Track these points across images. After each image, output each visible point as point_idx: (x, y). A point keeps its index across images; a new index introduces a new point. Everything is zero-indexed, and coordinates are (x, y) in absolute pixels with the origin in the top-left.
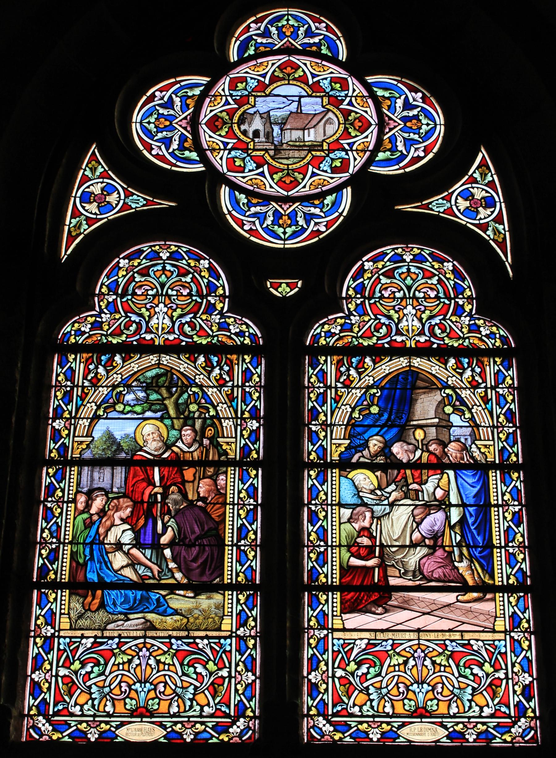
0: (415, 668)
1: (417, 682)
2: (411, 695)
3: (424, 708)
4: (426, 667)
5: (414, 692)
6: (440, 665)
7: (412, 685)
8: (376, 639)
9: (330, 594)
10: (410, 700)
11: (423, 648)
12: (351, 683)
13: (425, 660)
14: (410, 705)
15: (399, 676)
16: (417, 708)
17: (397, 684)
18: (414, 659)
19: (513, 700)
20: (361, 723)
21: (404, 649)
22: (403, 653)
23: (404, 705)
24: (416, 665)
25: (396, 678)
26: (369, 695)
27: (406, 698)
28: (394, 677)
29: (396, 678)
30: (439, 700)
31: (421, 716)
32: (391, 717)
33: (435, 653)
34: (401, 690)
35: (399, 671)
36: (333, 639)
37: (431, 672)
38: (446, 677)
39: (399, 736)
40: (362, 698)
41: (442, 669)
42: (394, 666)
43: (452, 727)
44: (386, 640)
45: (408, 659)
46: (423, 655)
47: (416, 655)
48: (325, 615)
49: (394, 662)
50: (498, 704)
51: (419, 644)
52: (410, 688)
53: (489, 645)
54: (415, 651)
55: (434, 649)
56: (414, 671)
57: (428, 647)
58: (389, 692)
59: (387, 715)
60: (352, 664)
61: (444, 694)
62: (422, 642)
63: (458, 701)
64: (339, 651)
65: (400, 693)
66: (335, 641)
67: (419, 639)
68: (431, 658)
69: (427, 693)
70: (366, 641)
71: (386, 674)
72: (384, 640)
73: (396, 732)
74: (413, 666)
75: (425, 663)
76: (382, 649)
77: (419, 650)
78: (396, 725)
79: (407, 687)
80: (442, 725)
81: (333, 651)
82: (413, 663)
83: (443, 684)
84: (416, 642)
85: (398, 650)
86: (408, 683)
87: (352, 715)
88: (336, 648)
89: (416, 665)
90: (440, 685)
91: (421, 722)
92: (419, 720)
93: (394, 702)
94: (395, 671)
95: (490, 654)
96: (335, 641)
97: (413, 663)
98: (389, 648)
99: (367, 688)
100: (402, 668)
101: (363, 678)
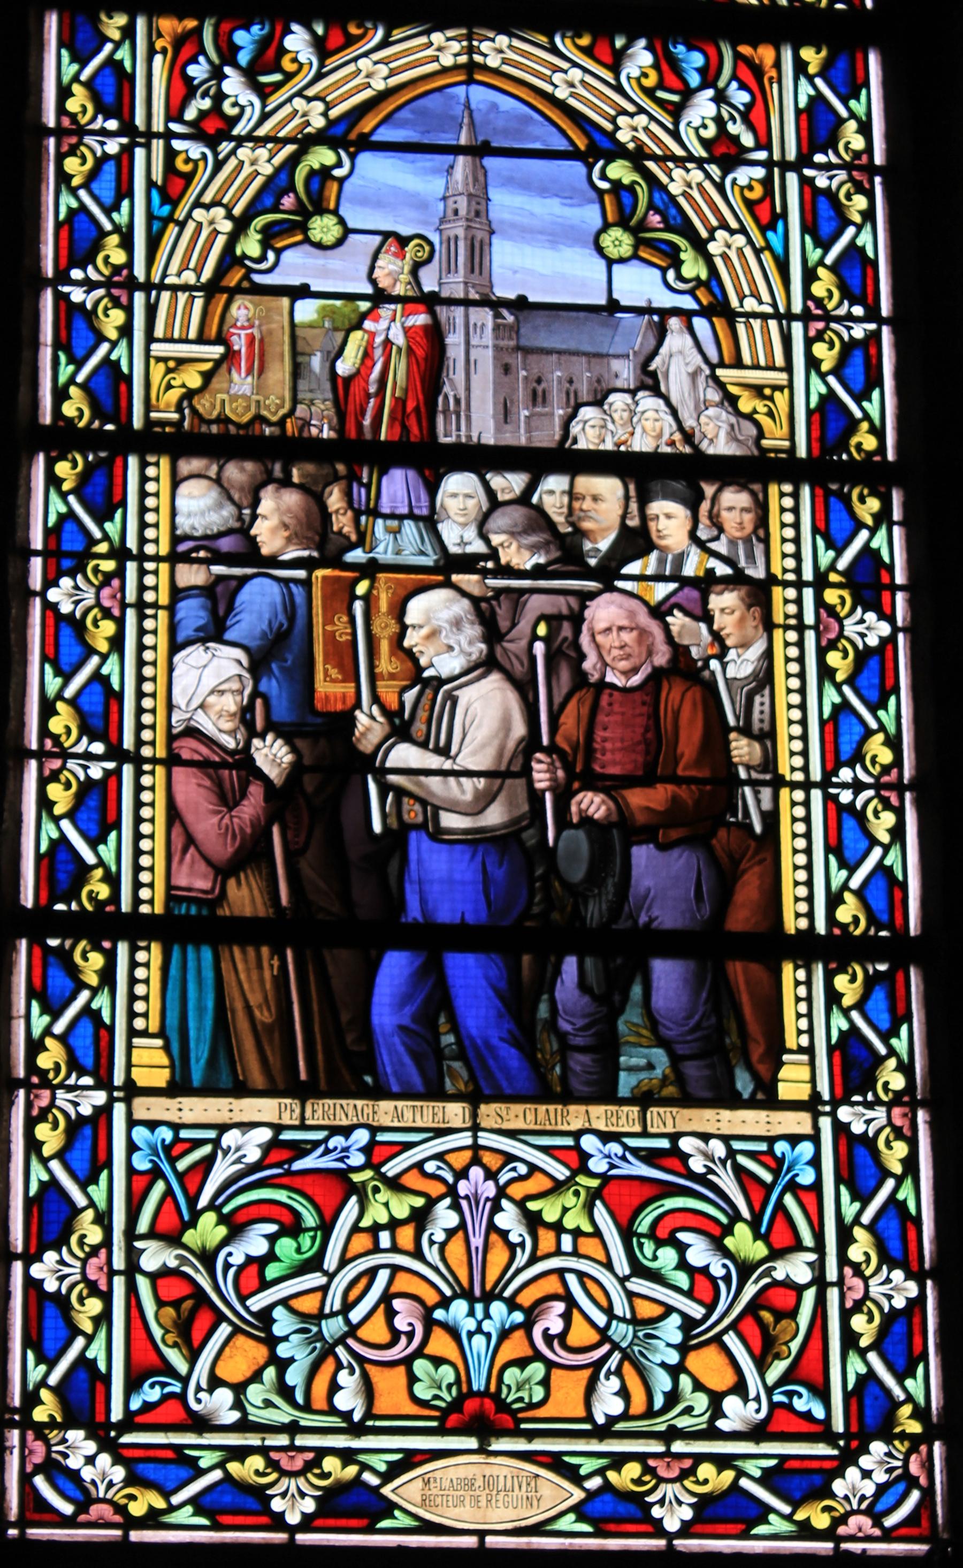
0: (458, 1239)
6: (558, 1228)
8: (303, 1127)
13: (497, 1208)
16: (465, 1395)
19: (843, 1371)
20: (240, 1454)
22: (411, 1180)
24: (462, 1225)
26: (272, 1342)
32: (358, 1430)
33: (537, 1184)
37: (521, 1258)
41: (567, 1242)
42: (375, 1229)
43: (601, 1472)
49: (377, 1214)
50: (781, 1382)
51: (476, 1147)
54: (462, 1174)
55: (533, 1169)
56: (456, 1249)
57: (510, 1158)
61: (572, 1340)
62: (485, 1139)
67: (475, 1128)
68: (520, 1204)
72: (335, 1130)
74: (450, 1233)
76: (327, 1163)
77: (476, 1173)
80: (555, 1462)
82: (452, 1219)
84: (465, 1139)
89: (462, 1225)
97: (452, 1219)
101: (250, 1280)
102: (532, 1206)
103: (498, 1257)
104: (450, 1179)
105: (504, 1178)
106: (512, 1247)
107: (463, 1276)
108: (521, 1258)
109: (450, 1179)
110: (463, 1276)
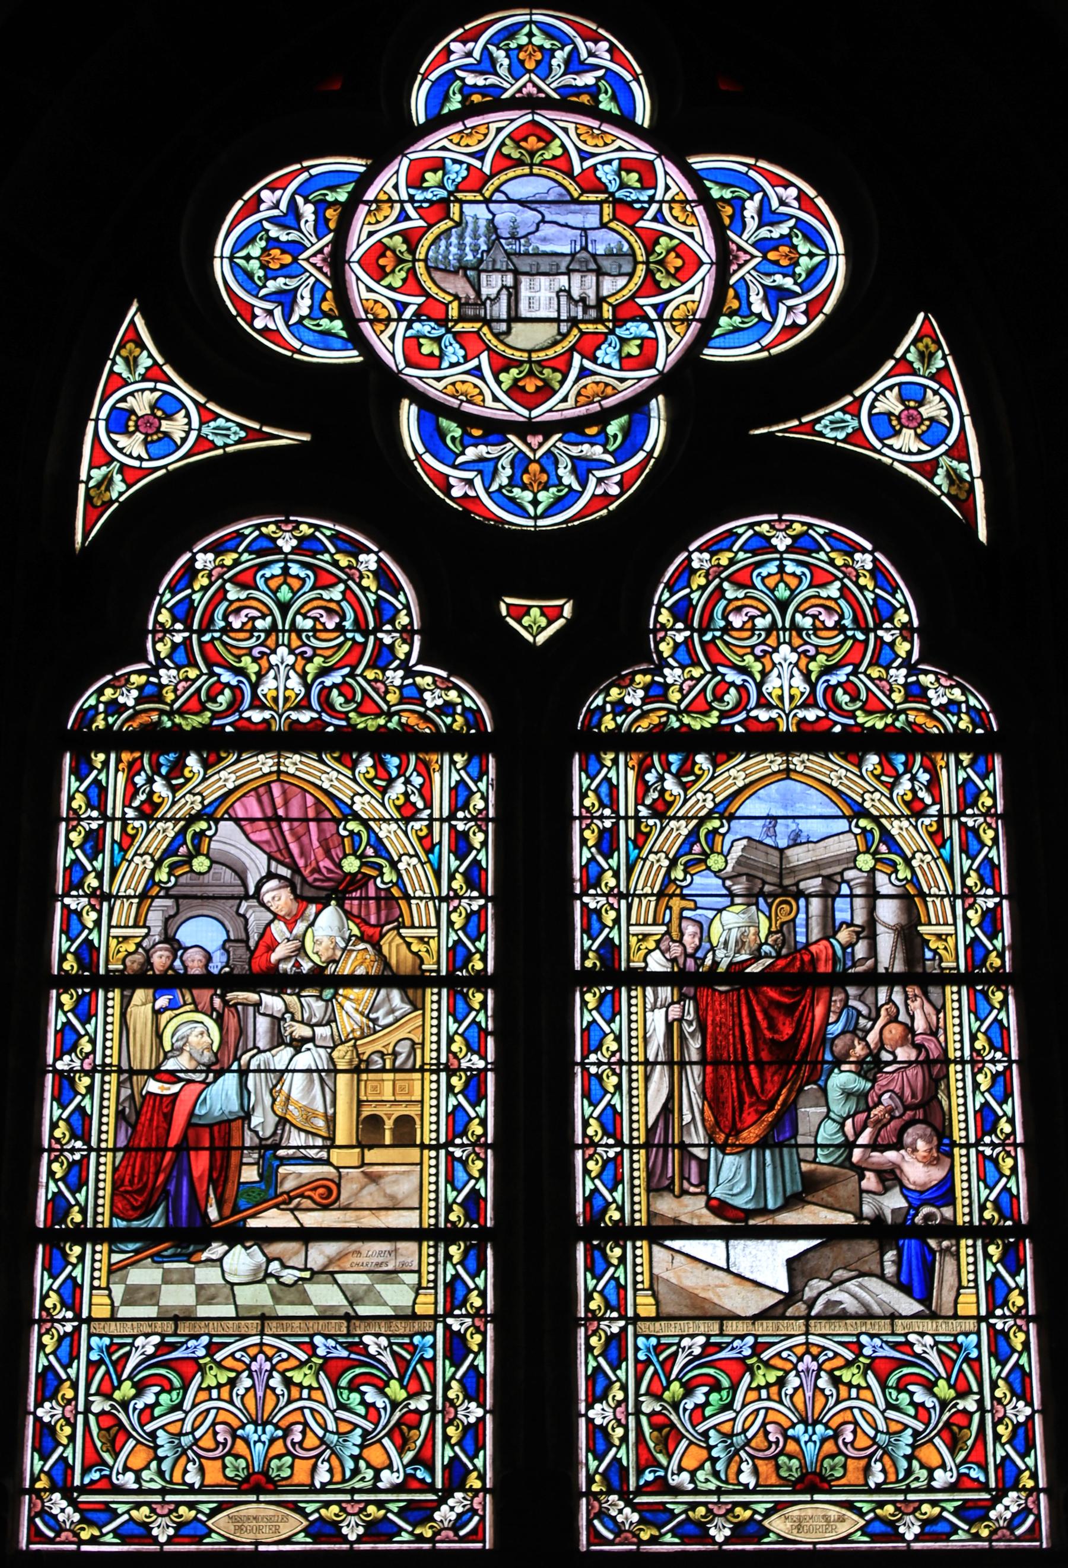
1: (803, 1421)
2: (791, 1447)
6: (849, 1385)
7: (793, 1426)
9: (629, 1244)
11: (815, 1350)
12: (673, 1425)
15: (767, 1409)
17: (764, 1425)
18: (798, 1375)
21: (779, 1354)
22: (776, 1362)
23: (778, 1467)
25: (762, 1412)
27: (781, 1453)
28: (757, 1410)
29: (762, 1412)
30: (847, 1457)
31: (812, 1490)
33: (838, 1362)
34: (772, 1438)
35: (769, 1399)
36: (636, 1336)
37: (832, 1401)
40: (694, 1457)
42: (759, 1388)
44: (742, 1337)
45: (787, 1373)
46: (814, 1366)
48: (621, 1288)
51: (807, 1343)
55: (836, 1354)
58: (748, 1442)
60: (675, 1386)
62: (812, 1339)
63: (886, 1459)
64: (648, 1362)
66: (641, 1341)
68: (830, 1373)
70: (701, 1340)
71: (744, 1406)
74: (796, 1390)
77: (807, 1358)
78: (761, 1508)
79: (784, 1431)
81: (637, 1361)
83: (856, 1423)
85: (765, 1356)
86: (786, 1424)
87: (677, 1491)
88: (642, 1356)
89: (801, 1385)
90: (851, 1427)
92: (807, 1497)
93: (758, 1462)
94: (760, 1399)
96: (641, 1341)
98: (747, 1352)
99: (705, 1434)
103: (820, 1400)
105: (822, 1359)
108: (832, 1401)
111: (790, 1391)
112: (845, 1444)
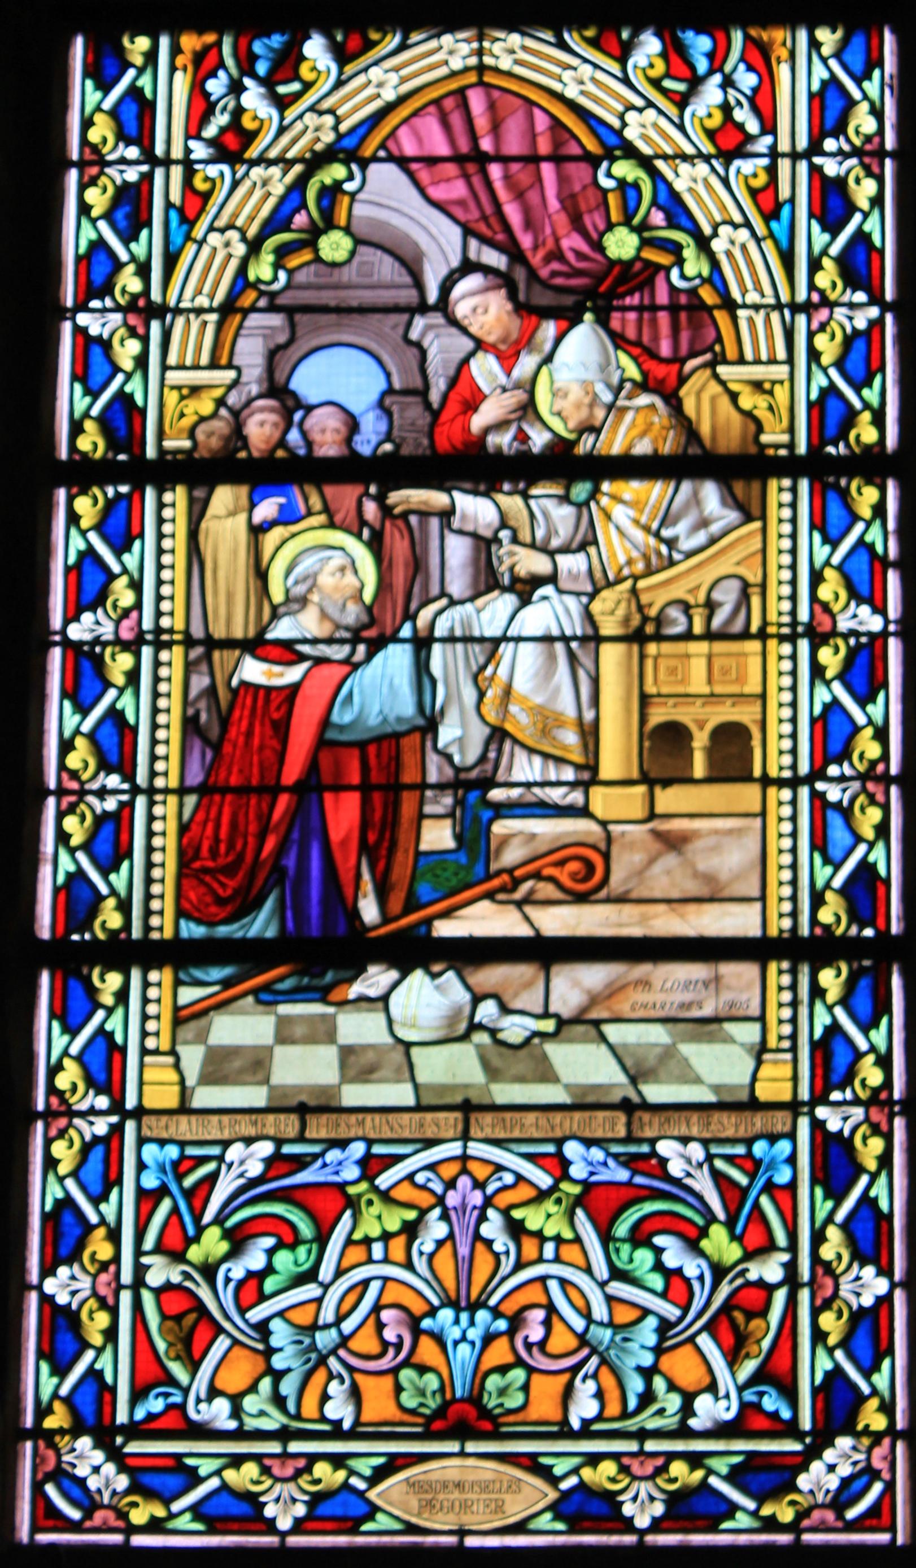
0: (447, 1249)
3: (475, 1398)
4: (489, 1243)
5: (439, 1339)
7: (432, 1312)
10: (423, 1369)
11: (481, 1172)
13: (482, 1218)
14: (420, 1391)
15: (386, 1279)
17: (377, 1308)
18: (445, 1217)
21: (410, 1177)
29: (375, 1287)
30: (531, 1370)
31: (462, 1432)
33: (525, 1192)
37: (507, 1265)
38: (563, 1282)
39: (373, 1510)
45: (423, 1212)
47: (452, 1199)
51: (464, 1158)
52: (426, 1323)
53: (730, 1159)
54: (451, 1184)
55: (520, 1178)
57: (499, 1168)
59: (337, 1432)
61: (555, 1345)
62: (475, 1149)
65: (385, 1344)
68: (506, 1212)
69: (489, 1339)
73: (361, 1494)
74: (440, 1243)
75: (485, 1230)
77: (464, 1182)
79: (414, 1323)
83: (551, 1309)
84: (454, 1149)
85: (384, 1180)
89: (451, 1236)
91: (462, 1454)
92: (453, 1447)
94: (370, 1261)
95: (734, 1195)
100: (397, 1246)
102: (517, 1214)
104: (438, 1187)
106: (497, 1256)
107: (450, 1284)
108: (507, 1265)
109: (438, 1187)
110: (450, 1284)
111: (429, 1247)
112: (528, 1346)
